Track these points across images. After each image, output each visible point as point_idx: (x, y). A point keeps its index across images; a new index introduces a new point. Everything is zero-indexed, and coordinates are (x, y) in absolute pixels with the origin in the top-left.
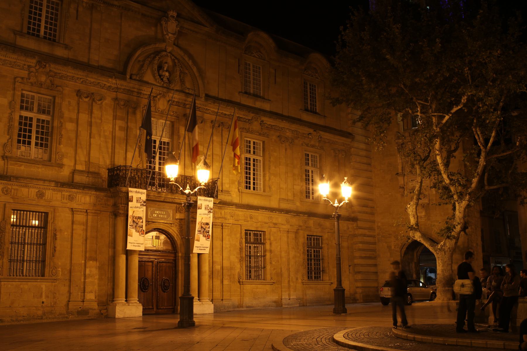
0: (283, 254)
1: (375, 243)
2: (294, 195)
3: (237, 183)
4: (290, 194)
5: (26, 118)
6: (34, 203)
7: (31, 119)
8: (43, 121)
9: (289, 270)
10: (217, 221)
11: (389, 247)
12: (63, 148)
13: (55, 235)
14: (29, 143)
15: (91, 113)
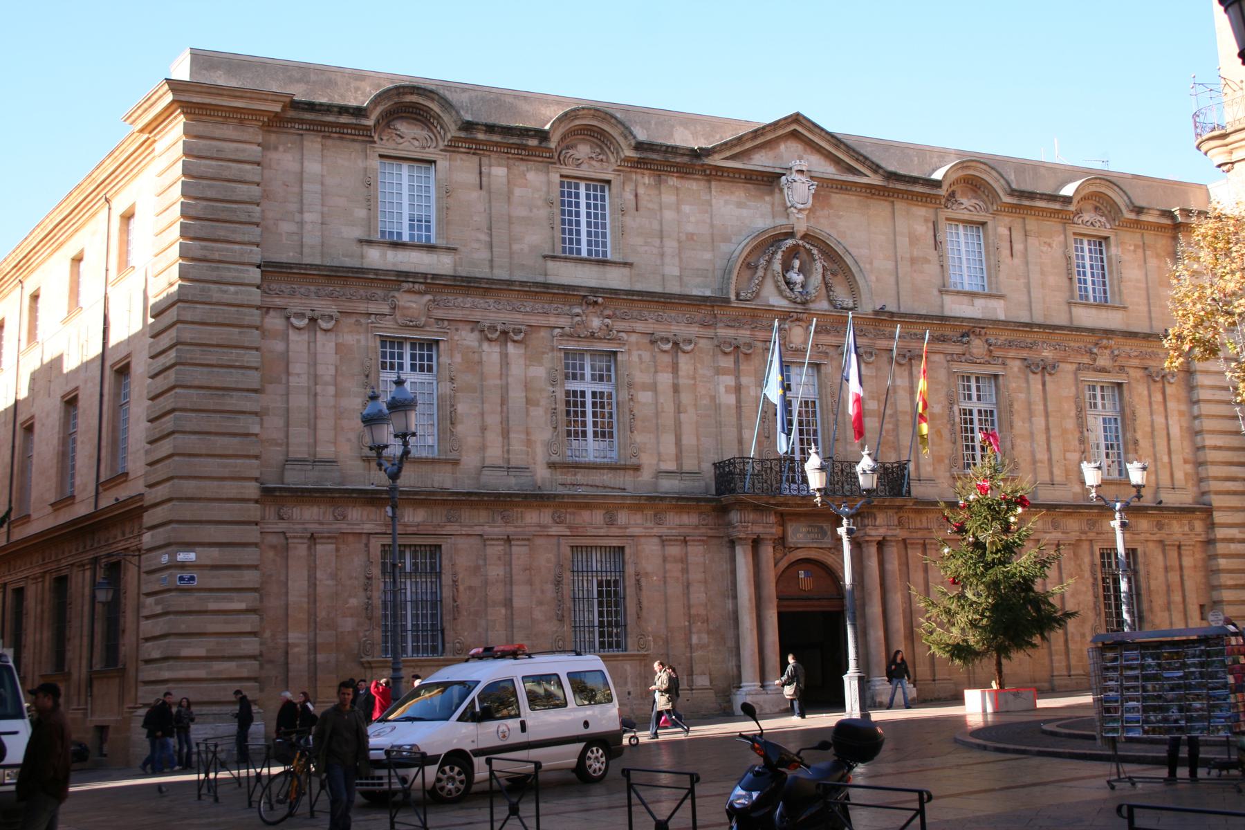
3: (947, 461)
5: (575, 392)
6: (602, 532)
7: (583, 394)
8: (602, 393)
12: (639, 438)
13: (638, 581)
14: (584, 434)
15: (675, 369)
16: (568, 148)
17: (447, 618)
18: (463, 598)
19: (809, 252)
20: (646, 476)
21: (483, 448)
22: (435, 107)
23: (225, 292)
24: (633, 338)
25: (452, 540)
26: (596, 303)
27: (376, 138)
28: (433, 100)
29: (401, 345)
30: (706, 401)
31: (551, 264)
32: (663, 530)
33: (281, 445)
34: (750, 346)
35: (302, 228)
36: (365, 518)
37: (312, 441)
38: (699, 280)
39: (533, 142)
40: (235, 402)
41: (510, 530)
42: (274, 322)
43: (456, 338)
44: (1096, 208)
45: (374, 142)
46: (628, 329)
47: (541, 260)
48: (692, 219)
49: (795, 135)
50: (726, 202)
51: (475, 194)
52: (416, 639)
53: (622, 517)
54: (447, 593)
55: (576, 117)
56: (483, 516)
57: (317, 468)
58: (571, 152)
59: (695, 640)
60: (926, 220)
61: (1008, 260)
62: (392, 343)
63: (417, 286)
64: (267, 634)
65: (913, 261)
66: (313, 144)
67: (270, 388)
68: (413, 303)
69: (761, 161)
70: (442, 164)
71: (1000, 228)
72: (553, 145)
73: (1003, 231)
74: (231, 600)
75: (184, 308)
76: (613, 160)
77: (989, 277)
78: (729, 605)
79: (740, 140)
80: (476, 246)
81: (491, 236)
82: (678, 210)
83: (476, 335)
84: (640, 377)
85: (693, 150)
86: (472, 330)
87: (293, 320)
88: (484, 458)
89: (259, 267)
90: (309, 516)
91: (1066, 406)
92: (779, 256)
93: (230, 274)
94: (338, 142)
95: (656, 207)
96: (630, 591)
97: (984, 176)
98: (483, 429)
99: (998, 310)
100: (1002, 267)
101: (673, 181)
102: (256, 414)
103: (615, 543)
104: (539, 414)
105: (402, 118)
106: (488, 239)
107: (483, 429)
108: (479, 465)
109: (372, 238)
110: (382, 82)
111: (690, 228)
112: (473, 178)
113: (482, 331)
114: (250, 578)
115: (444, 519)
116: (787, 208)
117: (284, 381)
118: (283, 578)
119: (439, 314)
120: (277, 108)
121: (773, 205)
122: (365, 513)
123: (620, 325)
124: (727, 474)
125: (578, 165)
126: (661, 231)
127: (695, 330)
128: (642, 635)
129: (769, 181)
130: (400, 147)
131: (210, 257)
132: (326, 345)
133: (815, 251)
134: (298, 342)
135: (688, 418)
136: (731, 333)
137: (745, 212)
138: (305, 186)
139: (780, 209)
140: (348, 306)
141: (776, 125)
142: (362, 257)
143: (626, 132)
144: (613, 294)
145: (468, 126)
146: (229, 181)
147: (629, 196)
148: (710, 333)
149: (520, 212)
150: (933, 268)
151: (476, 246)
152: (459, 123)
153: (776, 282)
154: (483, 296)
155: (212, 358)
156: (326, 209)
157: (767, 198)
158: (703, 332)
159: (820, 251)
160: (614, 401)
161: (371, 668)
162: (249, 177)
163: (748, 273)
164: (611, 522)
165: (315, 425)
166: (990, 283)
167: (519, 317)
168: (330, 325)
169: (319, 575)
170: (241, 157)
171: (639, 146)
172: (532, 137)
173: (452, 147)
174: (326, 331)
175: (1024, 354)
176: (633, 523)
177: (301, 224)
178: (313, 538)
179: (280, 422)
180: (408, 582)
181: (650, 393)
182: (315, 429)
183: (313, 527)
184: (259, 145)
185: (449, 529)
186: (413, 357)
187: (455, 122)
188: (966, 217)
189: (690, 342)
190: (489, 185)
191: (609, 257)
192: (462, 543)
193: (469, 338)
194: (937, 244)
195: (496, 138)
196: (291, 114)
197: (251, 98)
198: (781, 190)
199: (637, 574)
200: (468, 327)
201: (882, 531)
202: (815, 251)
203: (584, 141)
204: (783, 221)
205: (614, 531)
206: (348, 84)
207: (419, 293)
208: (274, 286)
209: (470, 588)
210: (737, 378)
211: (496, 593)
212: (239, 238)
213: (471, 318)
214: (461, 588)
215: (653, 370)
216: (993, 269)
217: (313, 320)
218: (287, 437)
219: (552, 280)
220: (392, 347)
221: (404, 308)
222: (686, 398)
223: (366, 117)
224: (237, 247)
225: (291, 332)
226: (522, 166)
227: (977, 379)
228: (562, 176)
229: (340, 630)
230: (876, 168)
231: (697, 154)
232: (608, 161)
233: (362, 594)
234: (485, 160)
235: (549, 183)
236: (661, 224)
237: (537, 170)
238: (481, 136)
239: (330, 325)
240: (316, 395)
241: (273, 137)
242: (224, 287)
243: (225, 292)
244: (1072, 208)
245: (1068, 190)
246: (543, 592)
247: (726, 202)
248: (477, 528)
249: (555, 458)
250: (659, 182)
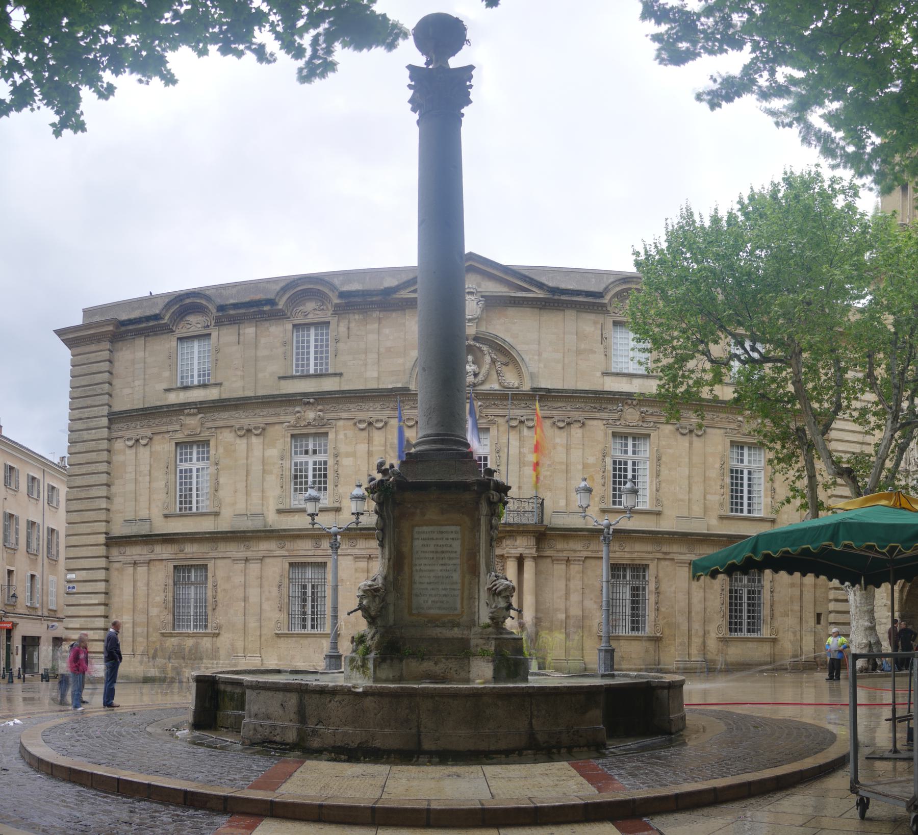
6: (310, 553)
18: (220, 596)
24: (341, 423)
31: (283, 382)
41: (249, 554)
46: (336, 417)
68: (192, 421)
86: (231, 432)
103: (320, 560)
104: (272, 480)
112: (234, 338)
119: (208, 425)
123: (329, 416)
132: (144, 453)
154: (236, 410)
181: (351, 459)
185: (211, 555)
200: (228, 430)
205: (319, 552)
207: (194, 414)
213: (229, 424)
214: (219, 590)
246: (270, 592)
249: (281, 507)
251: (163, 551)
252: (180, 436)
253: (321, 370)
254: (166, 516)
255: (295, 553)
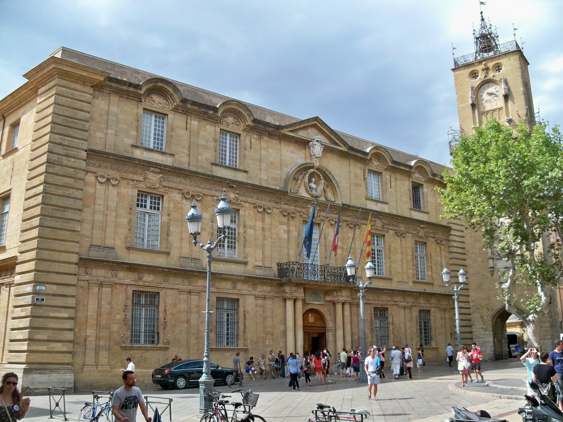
0: (402, 326)
1: (470, 314)
2: (408, 277)
4: (405, 277)
6: (230, 291)
9: (406, 338)
10: (354, 301)
11: (482, 317)
14: (224, 246)
16: (224, 117)
17: (161, 327)
18: (169, 318)
19: (319, 176)
20: (250, 267)
21: (181, 248)
22: (171, 90)
23: (69, 161)
24: (247, 205)
25: (164, 290)
26: (233, 187)
27: (143, 100)
28: (170, 87)
29: (146, 197)
30: (275, 236)
31: (214, 167)
32: (256, 293)
33: (88, 238)
34: (293, 213)
35: (107, 136)
36: (126, 277)
37: (103, 237)
38: (274, 182)
39: (211, 112)
40: (69, 214)
41: (191, 288)
42: (90, 178)
43: (171, 196)
44: (419, 172)
45: (142, 102)
47: (210, 165)
48: (273, 155)
49: (315, 126)
50: (287, 150)
51: (184, 132)
52: (145, 336)
53: (239, 286)
54: (161, 315)
55: (230, 104)
56: (179, 280)
57: (106, 251)
58: (225, 119)
59: (267, 343)
60: (361, 169)
61: (390, 189)
62: (142, 195)
63: (156, 169)
64: (77, 330)
65: (356, 185)
66: (115, 98)
67: (85, 210)
68: (154, 178)
69: (302, 134)
70: (171, 116)
71: (387, 176)
72: (219, 115)
73: (388, 177)
74: (61, 312)
75: (49, 166)
76: (242, 125)
77: (383, 195)
78: (282, 328)
79: (295, 124)
80: (183, 155)
81: (189, 151)
82: (267, 151)
83: (180, 195)
84: (249, 223)
85: (276, 126)
87: (99, 178)
88: (181, 253)
89: (86, 151)
90: (100, 273)
91: (408, 251)
92: (307, 176)
93: (73, 153)
94: (126, 100)
95: (259, 148)
96: (241, 319)
97: (383, 154)
98: (181, 239)
99: (386, 209)
100: (388, 192)
101: (266, 138)
102: (79, 221)
103: (235, 297)
105: (155, 93)
106: (188, 152)
107: (181, 239)
108: (179, 256)
109: (137, 145)
110: (147, 76)
111: (272, 159)
112: (184, 125)
113: (183, 194)
114: (71, 302)
115: (162, 280)
116: (311, 156)
117: (92, 207)
118: (86, 303)
119: (165, 184)
120: (102, 79)
121: (305, 154)
122: (126, 274)
123: (242, 198)
124: (283, 270)
125: (228, 125)
126: (260, 159)
127: (272, 204)
128: (245, 340)
129: (305, 144)
130: (153, 106)
131: (64, 143)
132: (113, 192)
133: (321, 176)
134: (100, 189)
135: (268, 243)
136: (286, 207)
137: (294, 155)
138: (110, 117)
139: (308, 156)
140: (125, 175)
141: (308, 120)
142: (133, 153)
143: (250, 113)
144: (240, 184)
145: (184, 101)
146: (76, 109)
147: (248, 142)
148: (278, 206)
149: (202, 142)
150: (363, 189)
151: (183, 155)
152: (181, 98)
153: (306, 187)
154: (185, 178)
155: (60, 192)
156: (118, 129)
157: (303, 151)
158: (275, 205)
159: (323, 176)
160: (237, 232)
161: (125, 349)
162: (85, 109)
163: (294, 182)
164: (234, 288)
165: (106, 230)
166: (383, 197)
167: (199, 190)
168: (116, 183)
169: (103, 303)
170: (83, 99)
171: (255, 121)
172: (211, 110)
173: (175, 110)
174: (114, 185)
175: (395, 228)
176: (244, 288)
177: (106, 134)
178: (101, 285)
179: (89, 227)
180: (144, 309)
181: (252, 230)
182: (105, 232)
183: (101, 279)
184: (91, 95)
185: (163, 285)
186: (151, 203)
187: (179, 98)
188: (375, 170)
189: (270, 209)
190: (190, 129)
191: (238, 167)
192: (169, 292)
193: (177, 197)
194: (365, 179)
195: (195, 108)
196: (108, 83)
197: (91, 72)
198: (309, 148)
199: (244, 312)
200: (177, 191)
201: (344, 298)
202: (321, 176)
203: (231, 116)
204: (309, 161)
206: (132, 75)
208: (91, 161)
209: (172, 313)
210: (288, 227)
211: (183, 317)
212: (78, 136)
213: (179, 187)
214: (168, 313)
215: (254, 220)
216: (384, 192)
217: (108, 180)
218: (92, 234)
219: (215, 174)
220: (142, 196)
221: (150, 179)
222: (267, 234)
223: (141, 89)
224: (77, 140)
225: (97, 184)
226: (204, 123)
227: (377, 236)
228: (221, 129)
229: (111, 330)
230: (345, 144)
231: (278, 128)
232: (240, 126)
233: (123, 313)
234: (189, 118)
235: (215, 131)
236: (260, 156)
237: (210, 125)
238: (189, 106)
239: (116, 183)
240: (107, 215)
241: (97, 93)
242: (69, 159)
243: (69, 161)
244: (413, 171)
245: (413, 163)
247: (287, 150)
248: (176, 286)
250: (260, 138)
251: (125, 277)
252: (142, 186)
253: (233, 165)
254: (129, 248)
255: (221, 291)
